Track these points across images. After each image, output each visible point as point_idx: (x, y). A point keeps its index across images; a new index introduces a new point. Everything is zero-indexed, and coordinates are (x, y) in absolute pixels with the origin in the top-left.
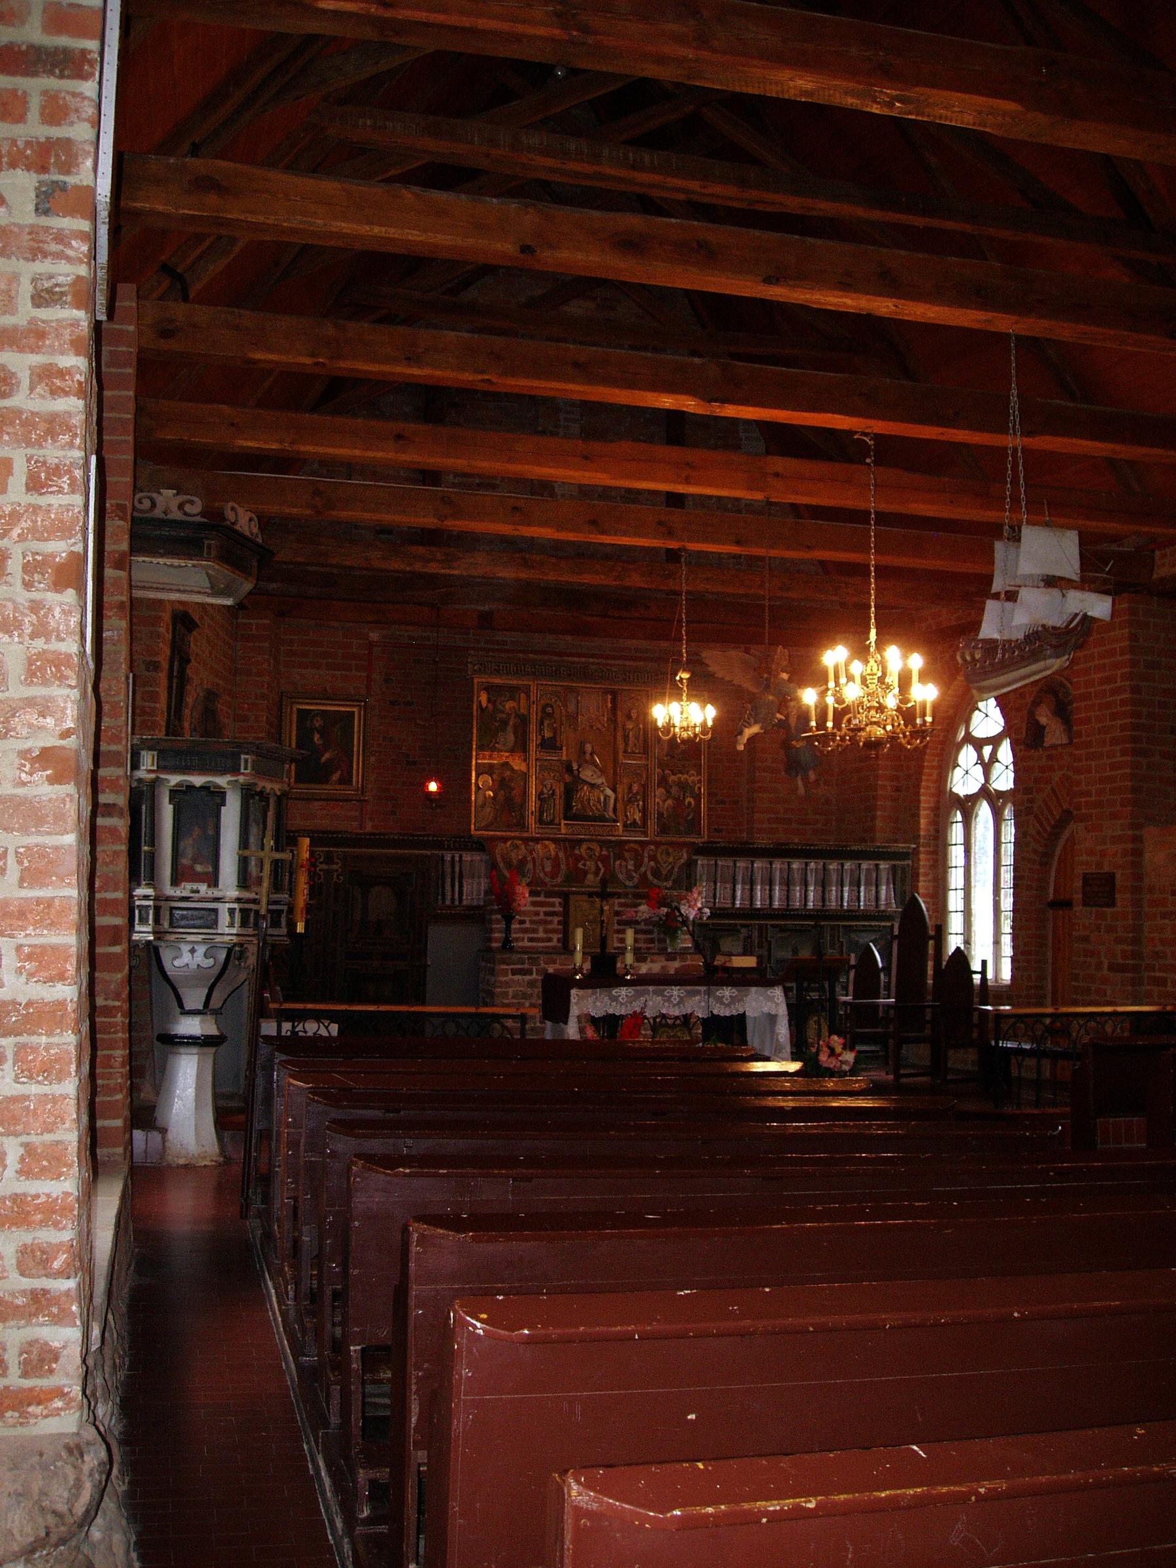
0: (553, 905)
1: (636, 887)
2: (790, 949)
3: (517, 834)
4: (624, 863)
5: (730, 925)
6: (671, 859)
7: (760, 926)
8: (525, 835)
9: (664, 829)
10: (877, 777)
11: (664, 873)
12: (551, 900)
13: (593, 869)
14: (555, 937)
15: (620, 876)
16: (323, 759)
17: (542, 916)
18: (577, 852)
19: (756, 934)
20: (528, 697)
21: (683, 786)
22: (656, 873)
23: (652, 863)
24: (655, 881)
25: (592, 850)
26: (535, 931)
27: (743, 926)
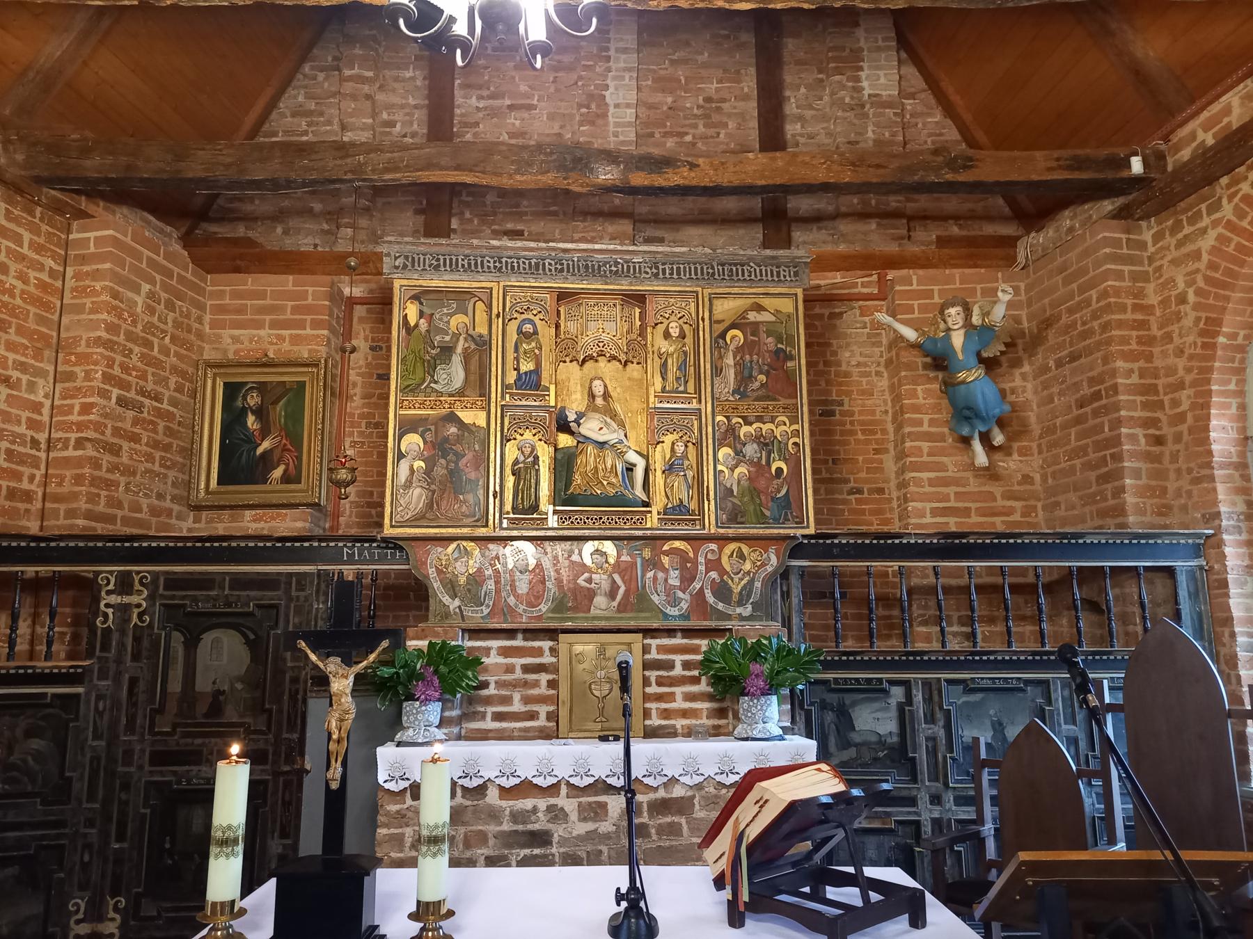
1: (685, 617)
2: (988, 723)
3: (465, 531)
4: (661, 575)
5: (869, 681)
6: (747, 566)
7: (927, 684)
8: (482, 532)
9: (735, 517)
10: (1117, 423)
11: (737, 589)
12: (536, 644)
13: (606, 586)
14: (543, 710)
15: (655, 598)
16: (260, 450)
17: (518, 674)
18: (575, 558)
19: (918, 697)
20: (490, 307)
21: (765, 443)
22: (722, 591)
23: (714, 575)
24: (720, 606)
25: (604, 554)
26: (507, 700)
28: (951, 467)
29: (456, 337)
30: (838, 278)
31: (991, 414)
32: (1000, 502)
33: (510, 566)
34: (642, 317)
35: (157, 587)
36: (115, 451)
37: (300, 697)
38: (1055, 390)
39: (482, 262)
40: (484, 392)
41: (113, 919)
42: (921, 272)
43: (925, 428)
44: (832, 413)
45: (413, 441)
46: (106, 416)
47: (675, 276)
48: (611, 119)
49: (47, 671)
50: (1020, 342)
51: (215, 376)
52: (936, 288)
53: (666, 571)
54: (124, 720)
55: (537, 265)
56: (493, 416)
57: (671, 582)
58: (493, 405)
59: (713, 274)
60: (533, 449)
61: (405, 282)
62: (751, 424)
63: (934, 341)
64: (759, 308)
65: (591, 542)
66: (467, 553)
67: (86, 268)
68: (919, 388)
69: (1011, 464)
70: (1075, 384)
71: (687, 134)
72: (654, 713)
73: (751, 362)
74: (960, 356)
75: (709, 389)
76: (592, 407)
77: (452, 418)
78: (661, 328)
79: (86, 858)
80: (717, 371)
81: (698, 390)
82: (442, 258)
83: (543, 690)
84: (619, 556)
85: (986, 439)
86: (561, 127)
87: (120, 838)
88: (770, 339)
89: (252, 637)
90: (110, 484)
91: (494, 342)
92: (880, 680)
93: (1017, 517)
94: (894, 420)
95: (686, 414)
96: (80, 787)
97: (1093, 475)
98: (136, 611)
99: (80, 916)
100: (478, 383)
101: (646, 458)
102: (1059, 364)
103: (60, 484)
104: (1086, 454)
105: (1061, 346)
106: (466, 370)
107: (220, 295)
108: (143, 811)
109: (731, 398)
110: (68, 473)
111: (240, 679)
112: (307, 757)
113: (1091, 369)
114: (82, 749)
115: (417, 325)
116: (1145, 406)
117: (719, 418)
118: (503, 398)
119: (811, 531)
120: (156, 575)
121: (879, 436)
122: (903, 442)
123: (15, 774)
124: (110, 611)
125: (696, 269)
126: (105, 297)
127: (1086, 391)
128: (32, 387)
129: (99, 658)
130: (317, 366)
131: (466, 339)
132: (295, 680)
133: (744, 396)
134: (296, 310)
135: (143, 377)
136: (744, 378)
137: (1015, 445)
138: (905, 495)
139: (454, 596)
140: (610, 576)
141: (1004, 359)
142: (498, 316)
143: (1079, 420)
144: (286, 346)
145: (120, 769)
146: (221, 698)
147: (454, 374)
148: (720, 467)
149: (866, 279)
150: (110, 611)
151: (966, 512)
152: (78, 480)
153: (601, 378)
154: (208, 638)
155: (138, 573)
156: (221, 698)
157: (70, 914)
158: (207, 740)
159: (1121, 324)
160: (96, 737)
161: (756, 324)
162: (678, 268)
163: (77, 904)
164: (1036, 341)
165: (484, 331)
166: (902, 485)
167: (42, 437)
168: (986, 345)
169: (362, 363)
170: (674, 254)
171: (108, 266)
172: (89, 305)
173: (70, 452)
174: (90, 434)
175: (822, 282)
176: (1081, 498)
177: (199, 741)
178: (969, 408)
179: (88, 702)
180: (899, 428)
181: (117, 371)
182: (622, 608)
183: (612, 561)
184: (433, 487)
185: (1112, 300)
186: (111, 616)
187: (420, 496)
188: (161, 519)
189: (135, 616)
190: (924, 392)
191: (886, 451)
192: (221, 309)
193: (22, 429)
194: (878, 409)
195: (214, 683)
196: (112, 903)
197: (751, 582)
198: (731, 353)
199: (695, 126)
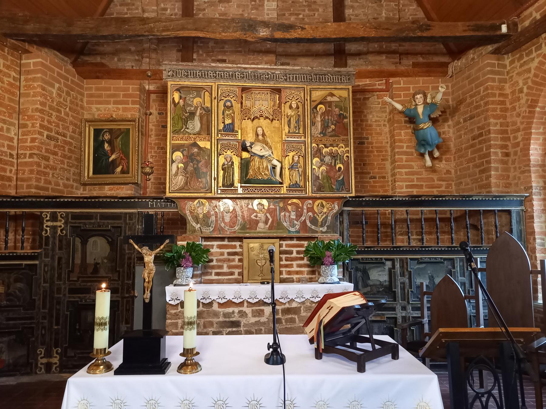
0: (235, 247)
2: (427, 276)
3: (202, 195)
4: (287, 214)
5: (376, 259)
6: (325, 210)
7: (401, 260)
9: (320, 189)
10: (489, 147)
11: (320, 220)
12: (233, 243)
13: (263, 219)
14: (237, 271)
15: (285, 224)
16: (111, 159)
17: (226, 256)
18: (250, 206)
19: (398, 265)
20: (211, 94)
21: (334, 156)
22: (314, 221)
23: (310, 214)
24: (313, 227)
25: (263, 205)
26: (221, 267)
27: (387, 260)
28: (415, 167)
29: (196, 108)
30: (368, 81)
31: (434, 143)
32: (436, 182)
33: (222, 210)
34: (280, 99)
35: (68, 219)
36: (47, 159)
37: (132, 265)
38: (462, 132)
39: (208, 73)
40: (209, 133)
41: (56, 357)
42: (405, 79)
43: (405, 149)
44: (363, 143)
45: (178, 155)
46: (42, 143)
47: (294, 80)
48: (266, 7)
49: (22, 254)
50: (448, 111)
51: (90, 126)
52: (411, 86)
53: (290, 212)
54: (56, 275)
55: (232, 75)
56: (213, 144)
57: (292, 217)
58: (213, 139)
59: (312, 79)
60: (231, 158)
61: (173, 83)
62: (327, 147)
63: (410, 110)
64: (332, 95)
65: (257, 200)
66: (203, 204)
67: (30, 77)
68: (402, 132)
69: (442, 166)
70: (472, 129)
71: (300, 14)
72: (284, 272)
73: (328, 119)
74: (421, 117)
75: (309, 132)
76: (257, 140)
77: (195, 145)
78: (288, 104)
79: (43, 332)
80: (313, 123)
81: (304, 132)
82: (189, 71)
83: (236, 263)
84: (269, 206)
85: (431, 154)
86: (243, 11)
87: (57, 324)
88: (337, 109)
89: (110, 240)
90: (45, 174)
91: (213, 111)
92: (381, 259)
93: (443, 189)
94: (391, 146)
95: (299, 143)
96: (39, 303)
97: (477, 170)
98: (59, 229)
99: (42, 355)
100: (206, 129)
101: (281, 163)
102: (465, 120)
103: (23, 174)
104: (475, 161)
105: (466, 113)
106: (201, 123)
107: (91, 89)
108: (66, 313)
109: (319, 136)
110: (27, 169)
111: (105, 258)
112: (136, 291)
113: (479, 123)
114: (39, 287)
115: (179, 103)
116: (502, 139)
117: (314, 145)
118: (218, 136)
119: (353, 195)
120: (67, 214)
121: (384, 153)
122: (395, 156)
123: (11, 297)
124: (48, 229)
125: (304, 77)
126: (39, 90)
127: (476, 132)
128: (8, 130)
129: (45, 249)
130: (135, 121)
131: (201, 109)
132: (130, 258)
133: (325, 135)
134: (124, 96)
135: (57, 126)
136: (325, 126)
137: (444, 157)
138: (395, 179)
139: (197, 223)
140: (265, 214)
141: (440, 119)
142: (215, 98)
143: (472, 146)
144: (121, 112)
145: (56, 295)
146: (98, 266)
147: (196, 125)
148: (314, 167)
149: (380, 82)
150: (48, 229)
151: (421, 187)
152: (31, 172)
153: (261, 127)
154: (91, 240)
155: (59, 212)
156: (98, 266)
157: (38, 355)
158: (92, 284)
159: (493, 103)
160: (45, 282)
161: (331, 102)
162: (296, 77)
163: (40, 351)
164: (455, 110)
165: (209, 106)
166: (393, 175)
167: (14, 153)
168: (432, 112)
169: (154, 120)
170: (295, 70)
171: (39, 75)
172: (32, 93)
173: (27, 160)
174: (36, 152)
175: (360, 84)
176: (471, 180)
177: (89, 284)
178: (424, 140)
179: (41, 267)
180: (393, 149)
181: (46, 123)
182: (270, 228)
183: (266, 208)
184: (187, 175)
185: (490, 91)
186: (49, 231)
187: (182, 179)
188: (69, 189)
189: (59, 231)
190: (405, 134)
191: (387, 160)
192: (91, 96)
193: (5, 149)
194: (384, 141)
195: (95, 259)
196: (55, 350)
197: (327, 217)
198: (319, 116)
199: (304, 11)
